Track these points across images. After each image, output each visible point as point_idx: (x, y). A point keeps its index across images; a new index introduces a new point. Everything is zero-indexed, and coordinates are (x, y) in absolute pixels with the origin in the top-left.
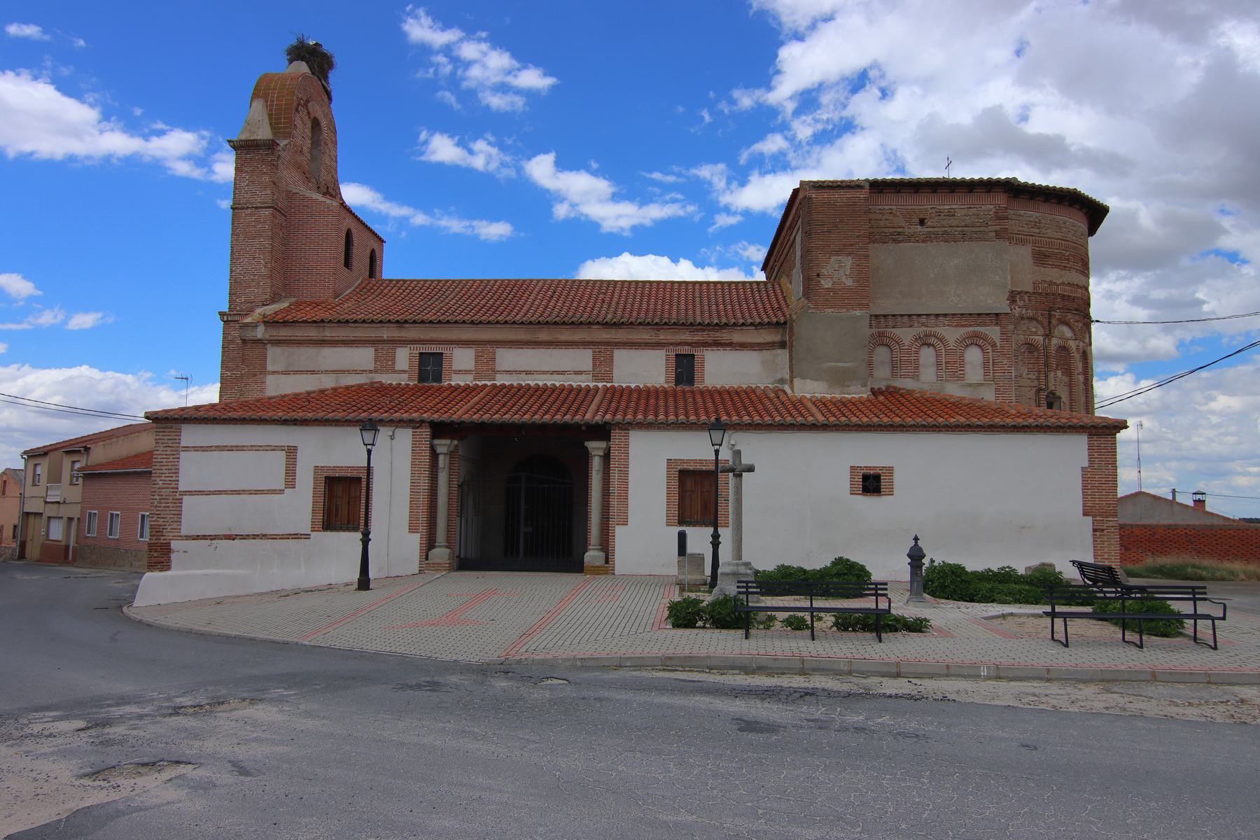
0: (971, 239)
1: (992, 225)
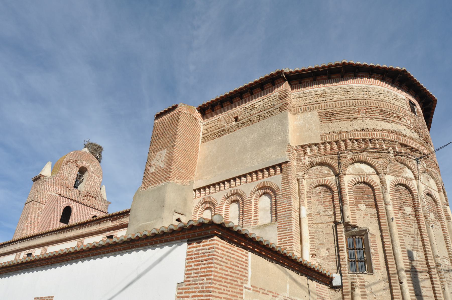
0: (264, 118)
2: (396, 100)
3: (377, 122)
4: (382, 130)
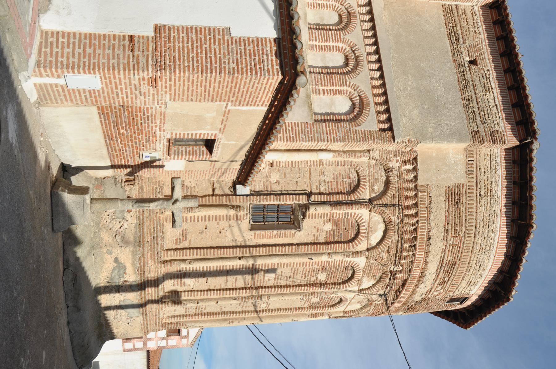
0: (466, 106)
2: (469, 283)
3: (439, 257)
4: (426, 262)
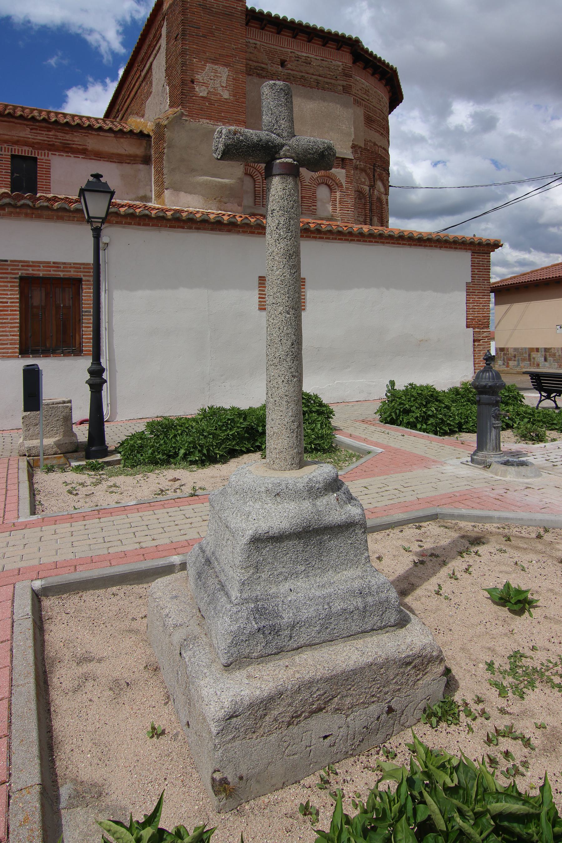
1: (340, 80)
